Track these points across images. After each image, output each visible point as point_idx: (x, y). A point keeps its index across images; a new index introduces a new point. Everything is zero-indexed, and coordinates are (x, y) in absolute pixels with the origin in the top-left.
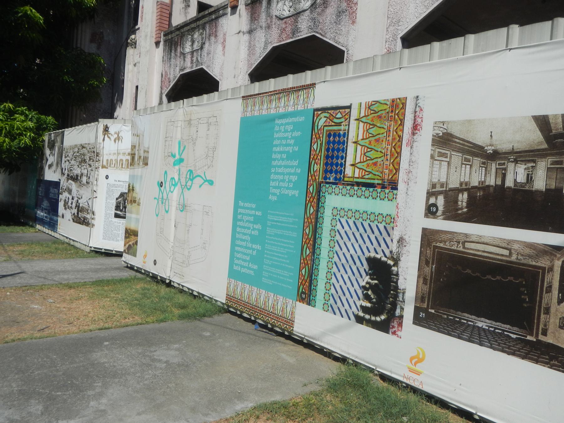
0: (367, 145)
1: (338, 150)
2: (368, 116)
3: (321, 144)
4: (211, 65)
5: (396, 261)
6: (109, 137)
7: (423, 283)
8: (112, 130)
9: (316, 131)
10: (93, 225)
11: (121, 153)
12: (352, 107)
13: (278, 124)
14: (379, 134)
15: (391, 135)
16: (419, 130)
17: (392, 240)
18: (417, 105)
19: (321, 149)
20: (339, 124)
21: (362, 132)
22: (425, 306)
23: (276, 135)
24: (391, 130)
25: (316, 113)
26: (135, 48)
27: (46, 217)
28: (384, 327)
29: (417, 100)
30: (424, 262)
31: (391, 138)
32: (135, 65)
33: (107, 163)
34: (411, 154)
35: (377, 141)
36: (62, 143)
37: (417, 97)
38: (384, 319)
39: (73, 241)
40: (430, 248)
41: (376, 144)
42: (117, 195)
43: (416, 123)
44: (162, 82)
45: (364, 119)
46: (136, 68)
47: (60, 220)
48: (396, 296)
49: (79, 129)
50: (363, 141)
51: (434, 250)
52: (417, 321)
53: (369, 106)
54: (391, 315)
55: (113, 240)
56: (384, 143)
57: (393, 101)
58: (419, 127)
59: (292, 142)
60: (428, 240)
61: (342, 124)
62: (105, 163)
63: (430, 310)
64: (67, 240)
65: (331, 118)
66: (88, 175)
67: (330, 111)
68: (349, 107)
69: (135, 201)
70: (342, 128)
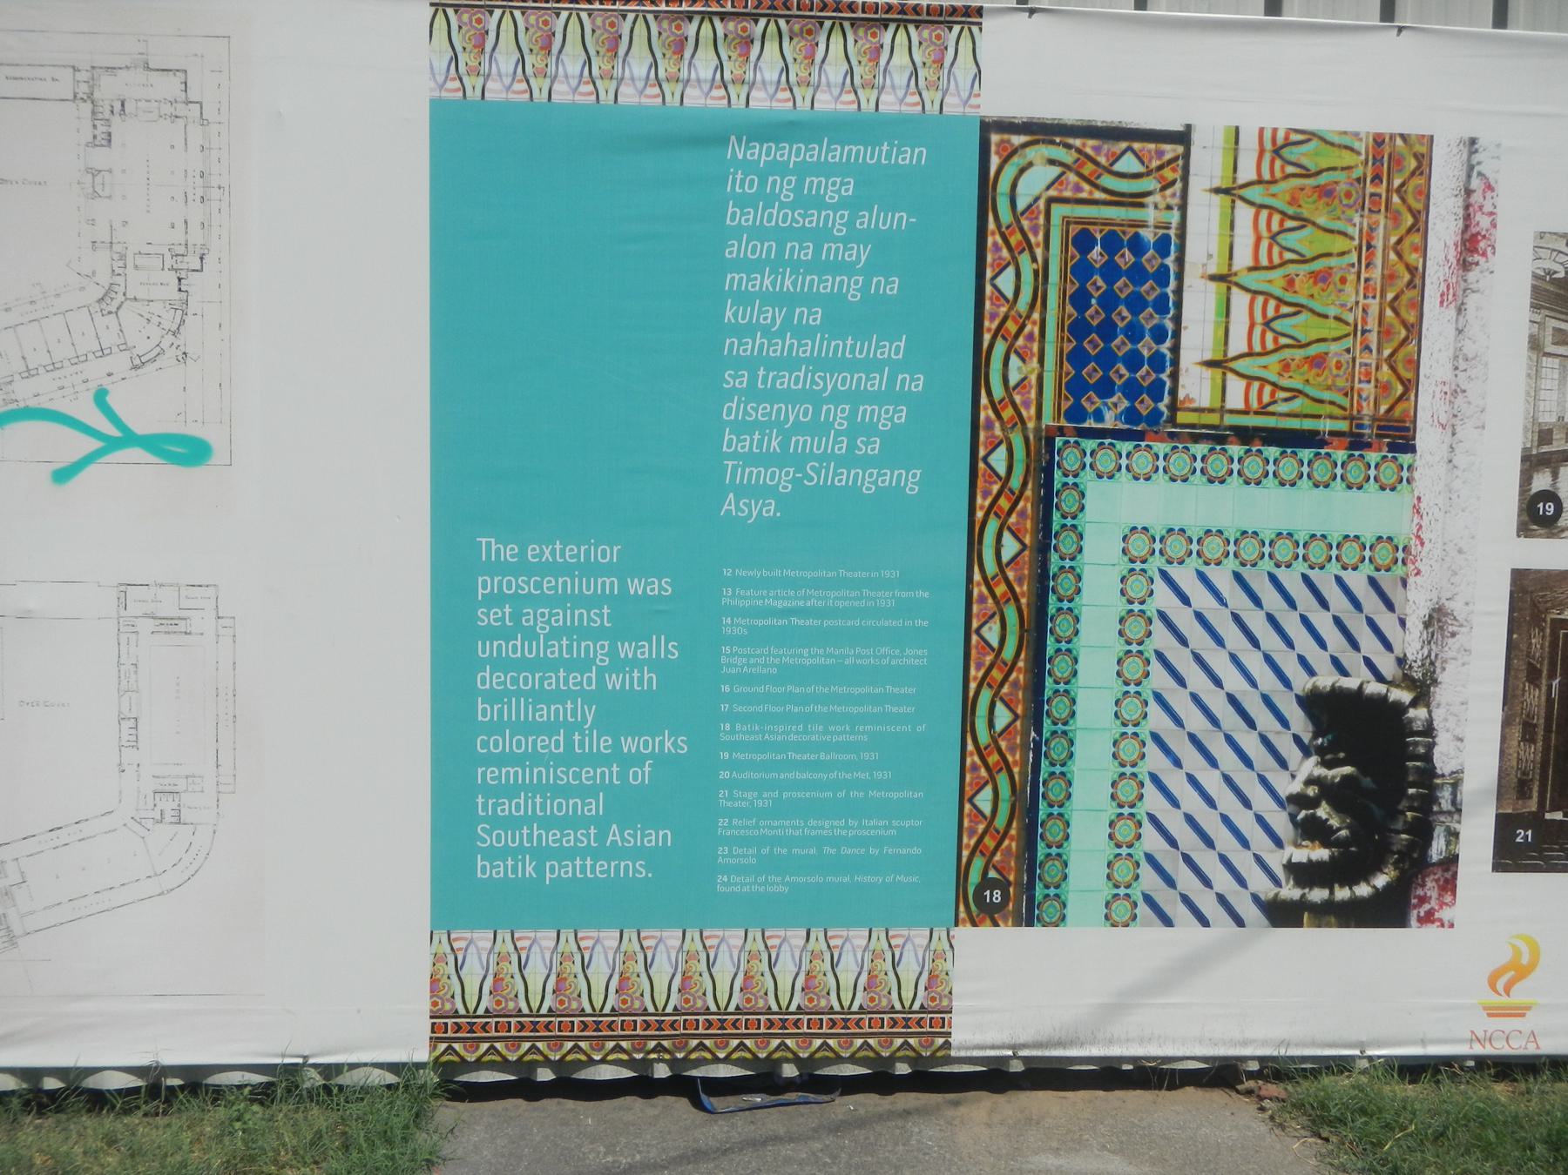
0: (1278, 292)
1: (1136, 304)
2: (1273, 182)
3: (1042, 276)
5: (1423, 690)
7: (1523, 739)
9: (1006, 216)
12: (1196, 137)
13: (749, 167)
14: (1329, 255)
15: (1378, 260)
16: (1484, 254)
17: (1403, 623)
18: (1471, 168)
19: (1039, 298)
20: (1136, 200)
21: (1251, 240)
22: (1533, 805)
23: (734, 216)
24: (1379, 243)
25: (995, 138)
28: (1388, 911)
29: (1472, 152)
30: (1523, 676)
31: (1376, 274)
34: (1460, 332)
35: (1321, 277)
37: (1473, 141)
38: (1388, 887)
40: (1542, 630)
41: (1316, 290)
43: (1474, 230)
45: (1255, 193)
48: (1428, 800)
50: (1255, 274)
51: (1554, 635)
52: (1508, 856)
53: (1278, 147)
54: (1415, 865)
56: (1349, 288)
57: (1379, 141)
58: (1482, 245)
59: (860, 254)
60: (1534, 605)
61: (1149, 200)
63: (1548, 816)
65: (1087, 170)
67: (1078, 142)
68: (1183, 137)
70: (1150, 215)
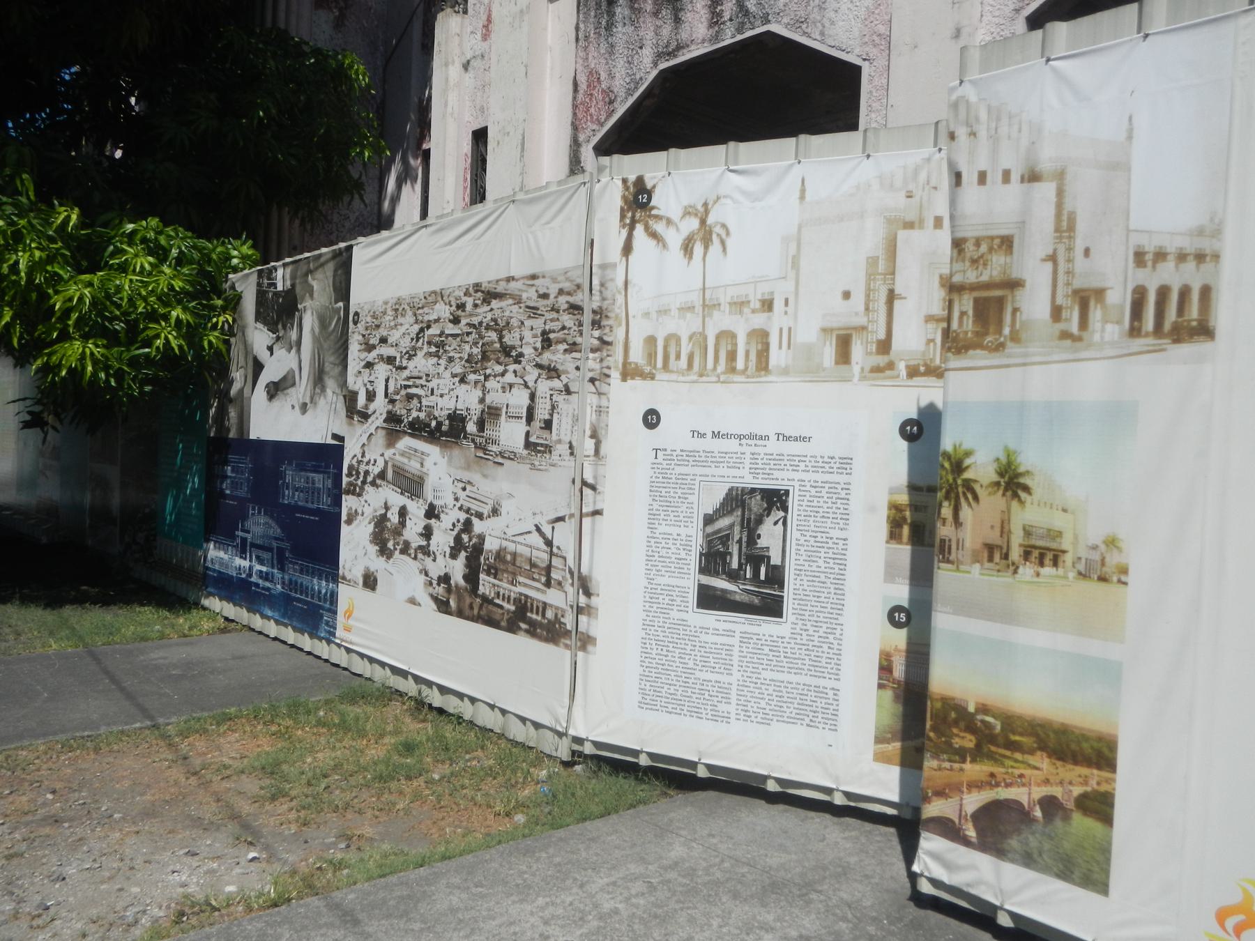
4: (815, 15)
6: (654, 235)
8: (666, 200)
10: (586, 641)
11: (724, 299)
26: (465, 12)
27: (265, 577)
32: (466, 66)
33: (651, 356)
36: (342, 290)
39: (444, 690)
42: (712, 499)
44: (575, 107)
46: (471, 73)
47: (347, 595)
49: (477, 214)
55: (696, 713)
62: (637, 355)
64: (409, 687)
66: (542, 413)
69: (1044, 553)
